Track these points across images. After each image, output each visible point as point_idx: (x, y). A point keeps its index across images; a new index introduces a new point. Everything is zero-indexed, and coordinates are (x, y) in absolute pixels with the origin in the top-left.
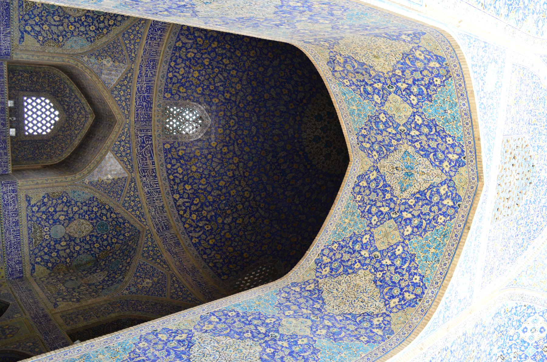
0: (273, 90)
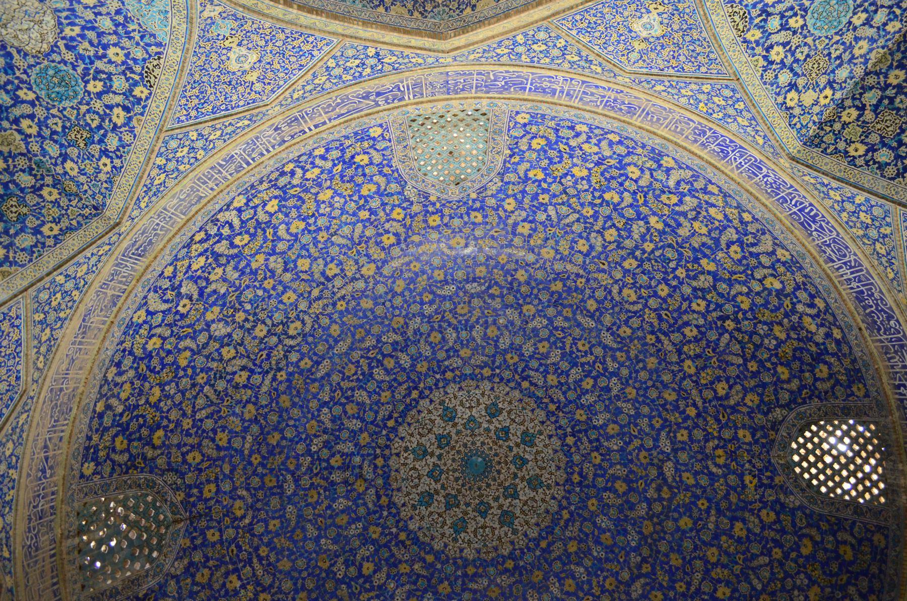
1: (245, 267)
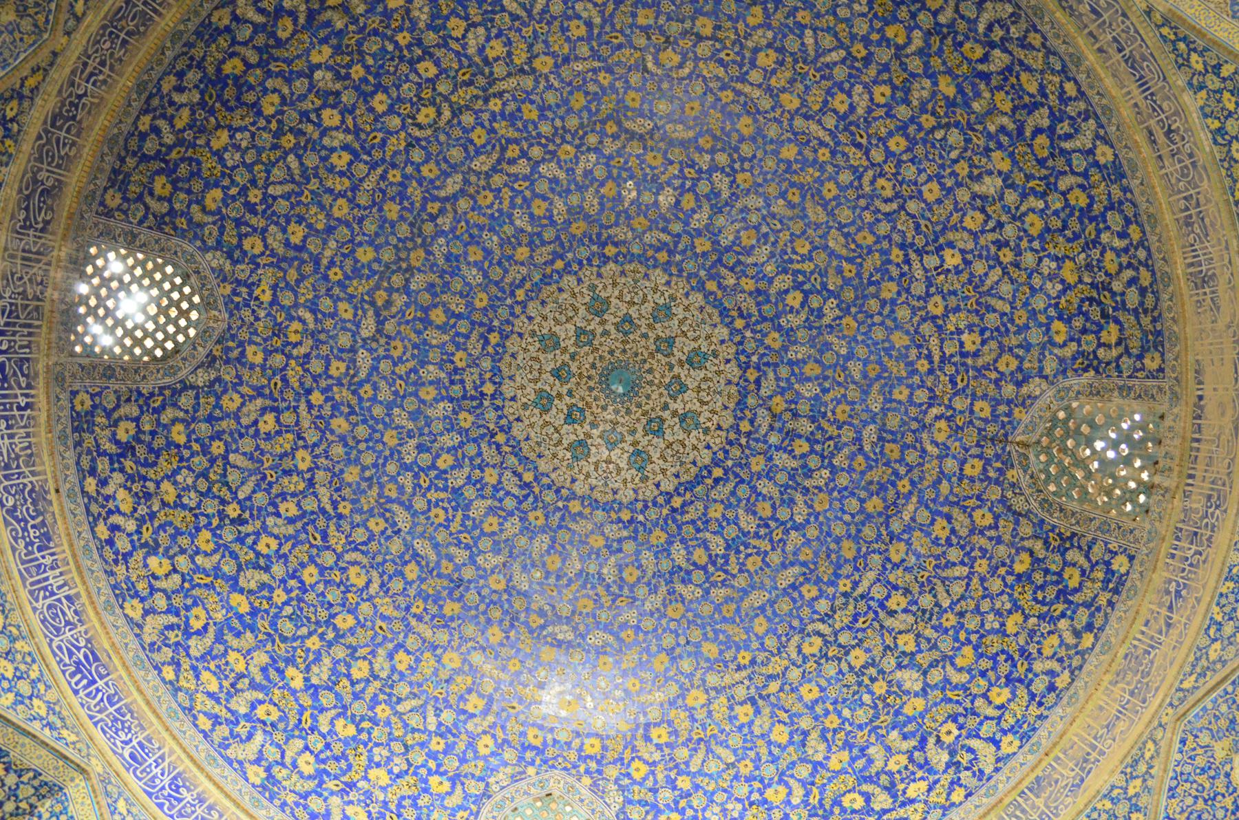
0: (480, 560)
1: (858, 758)
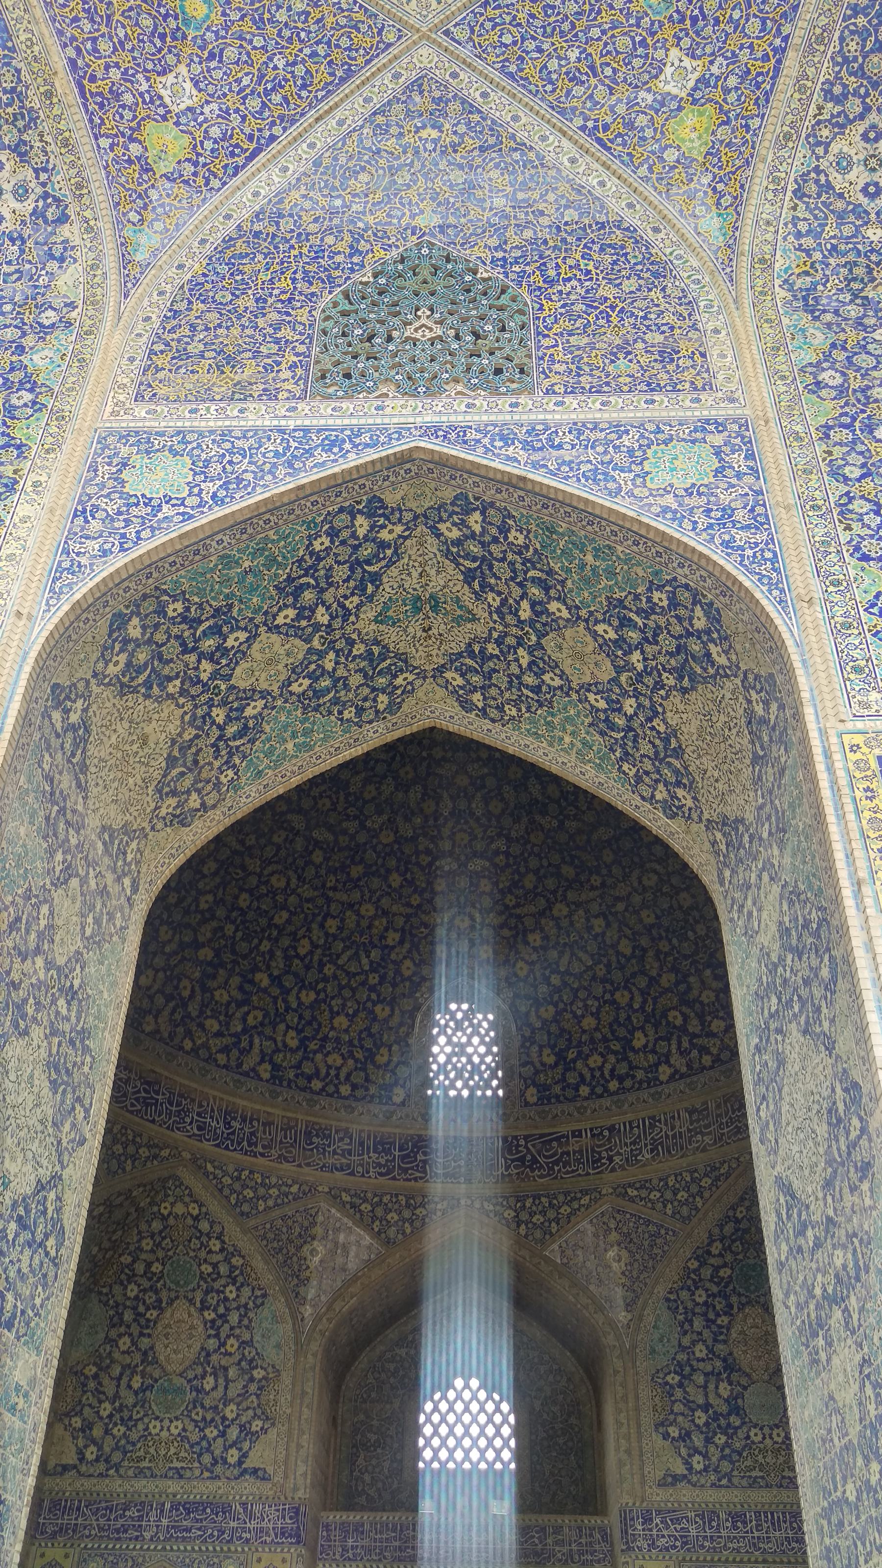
0: (368, 824)
